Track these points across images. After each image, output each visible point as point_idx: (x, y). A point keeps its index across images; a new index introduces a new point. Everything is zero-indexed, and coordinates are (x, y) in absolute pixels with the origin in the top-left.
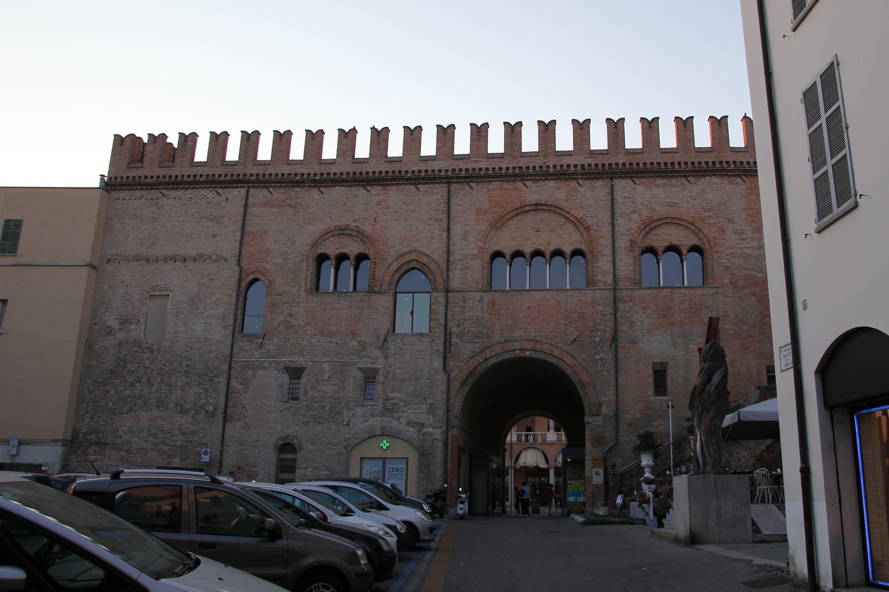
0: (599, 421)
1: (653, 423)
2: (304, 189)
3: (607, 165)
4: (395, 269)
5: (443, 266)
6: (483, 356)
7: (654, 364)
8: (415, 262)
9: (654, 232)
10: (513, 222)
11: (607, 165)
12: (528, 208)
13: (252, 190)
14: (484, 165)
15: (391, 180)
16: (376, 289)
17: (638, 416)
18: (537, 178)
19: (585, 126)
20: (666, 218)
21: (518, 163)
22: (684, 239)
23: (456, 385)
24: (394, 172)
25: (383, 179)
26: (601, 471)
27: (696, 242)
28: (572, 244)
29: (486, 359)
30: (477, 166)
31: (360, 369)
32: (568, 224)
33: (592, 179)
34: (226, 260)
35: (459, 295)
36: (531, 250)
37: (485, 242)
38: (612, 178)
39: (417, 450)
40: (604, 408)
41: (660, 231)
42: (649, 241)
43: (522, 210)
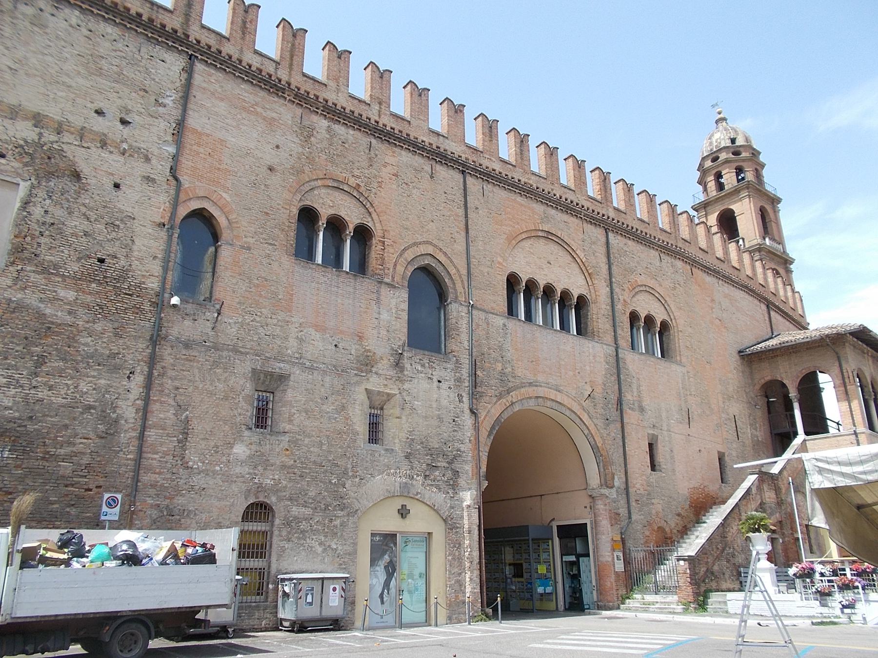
1: (653, 501)
2: (282, 101)
5: (464, 272)
10: (527, 244)
12: (540, 234)
13: (199, 67)
16: (386, 280)
17: (642, 491)
23: (484, 433)
26: (621, 555)
29: (512, 403)
31: (366, 389)
34: (147, 159)
39: (445, 521)
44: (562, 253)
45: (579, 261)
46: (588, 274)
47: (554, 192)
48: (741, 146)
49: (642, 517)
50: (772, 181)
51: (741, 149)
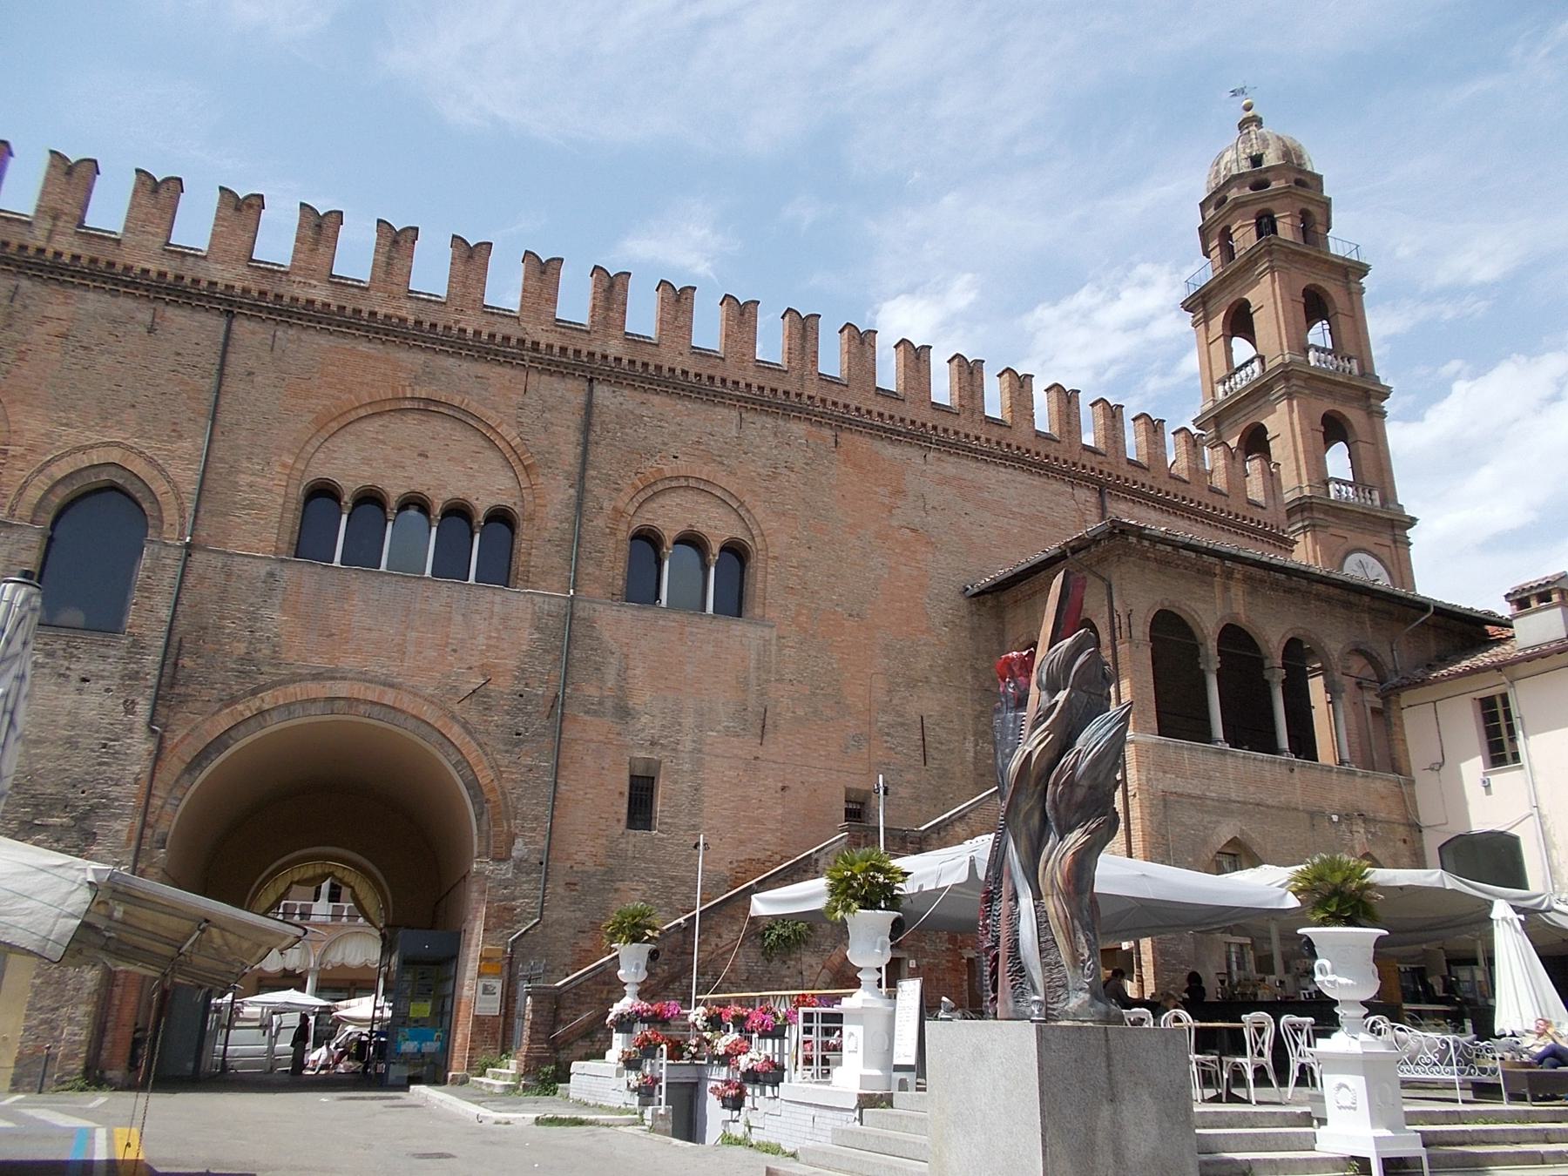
0: (506, 871)
1: (618, 885)
3: (584, 352)
4: (59, 475)
6: (255, 704)
7: (632, 761)
8: (113, 470)
9: (661, 500)
11: (584, 352)
12: (407, 404)
14: (321, 294)
15: (83, 275)
17: (590, 866)
18: (438, 348)
19: (549, 270)
20: (687, 478)
21: (400, 308)
22: (718, 528)
23: (174, 765)
24: (94, 261)
25: (63, 269)
27: (739, 533)
28: (492, 494)
30: (303, 294)
32: (490, 454)
33: (552, 374)
35: (218, 561)
36: (403, 491)
37: (297, 458)
38: (591, 380)
40: (519, 843)
41: (670, 500)
42: (650, 516)
43: (393, 408)
44: (459, 433)
45: (501, 444)
46: (521, 463)
47: (462, 325)
48: (1268, 169)
49: (578, 914)
50: (1344, 236)
51: (1269, 176)
